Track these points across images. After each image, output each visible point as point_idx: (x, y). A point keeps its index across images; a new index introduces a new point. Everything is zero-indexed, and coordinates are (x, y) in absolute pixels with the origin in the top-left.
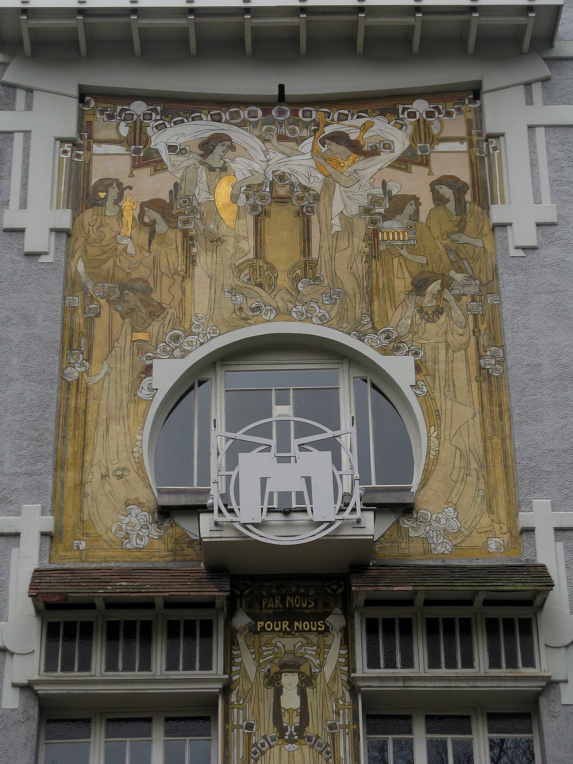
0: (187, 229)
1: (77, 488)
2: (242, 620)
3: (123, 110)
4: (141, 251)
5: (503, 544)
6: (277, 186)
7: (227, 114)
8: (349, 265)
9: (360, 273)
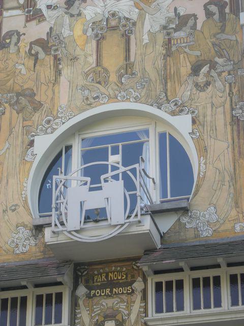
2: (82, 291)
4: (29, 71)
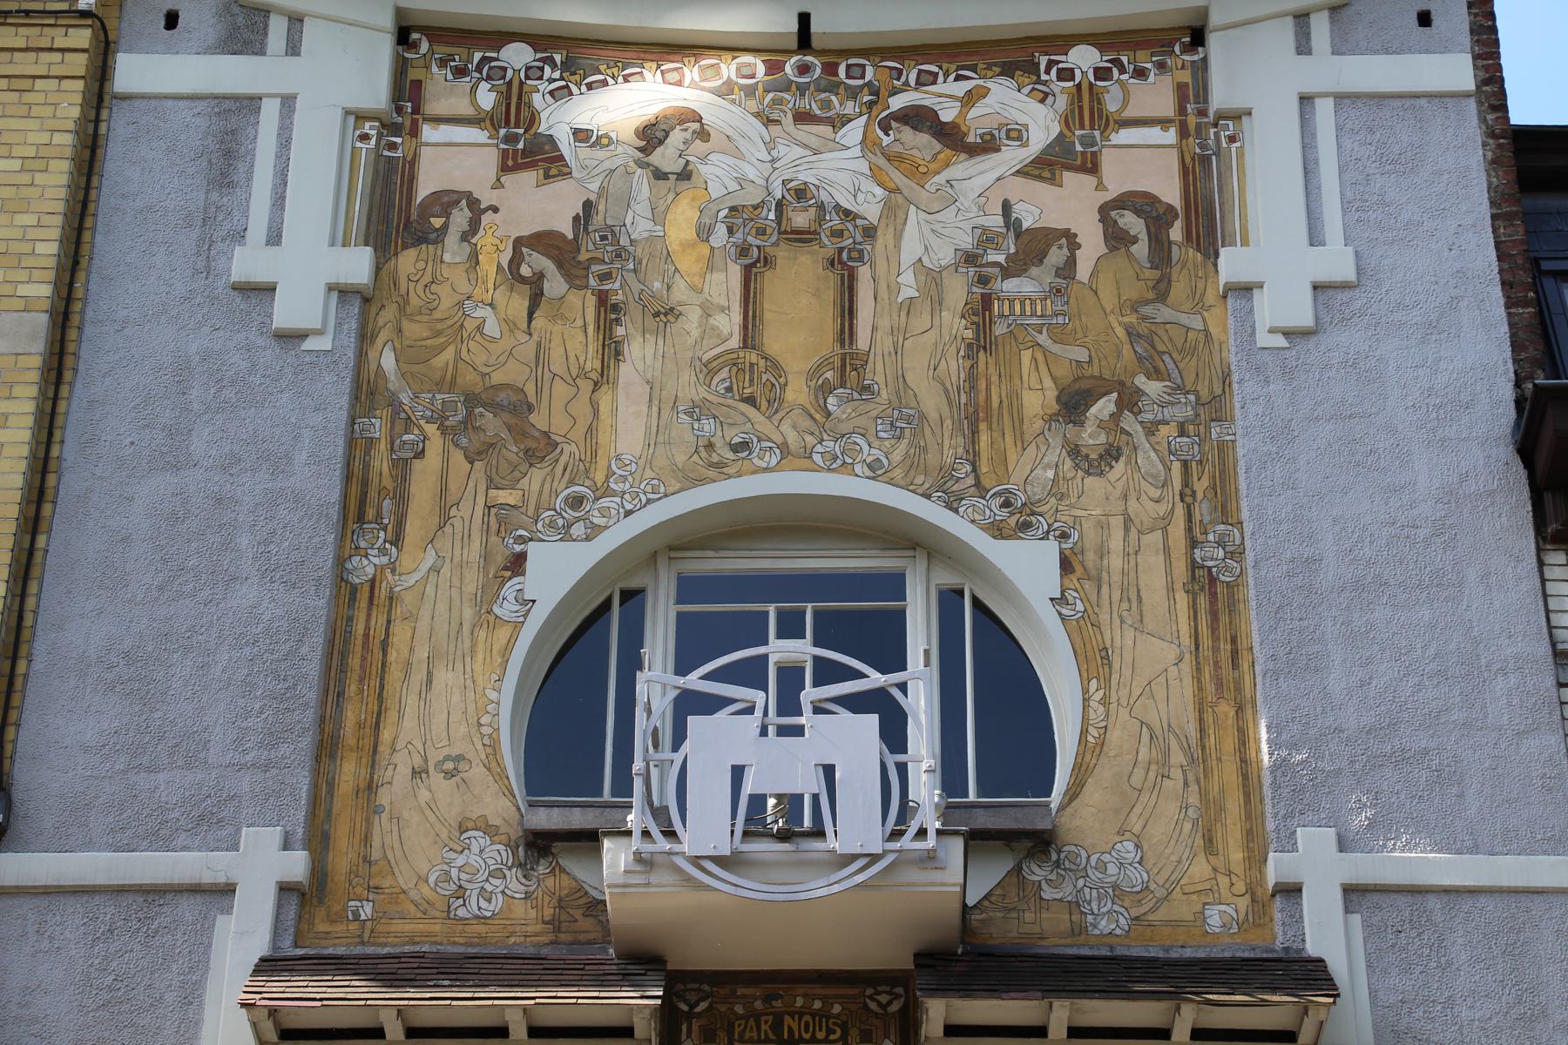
0: (608, 291)
1: (360, 795)
3: (484, 60)
5: (1235, 917)
6: (790, 209)
8: (932, 363)
9: (954, 379)
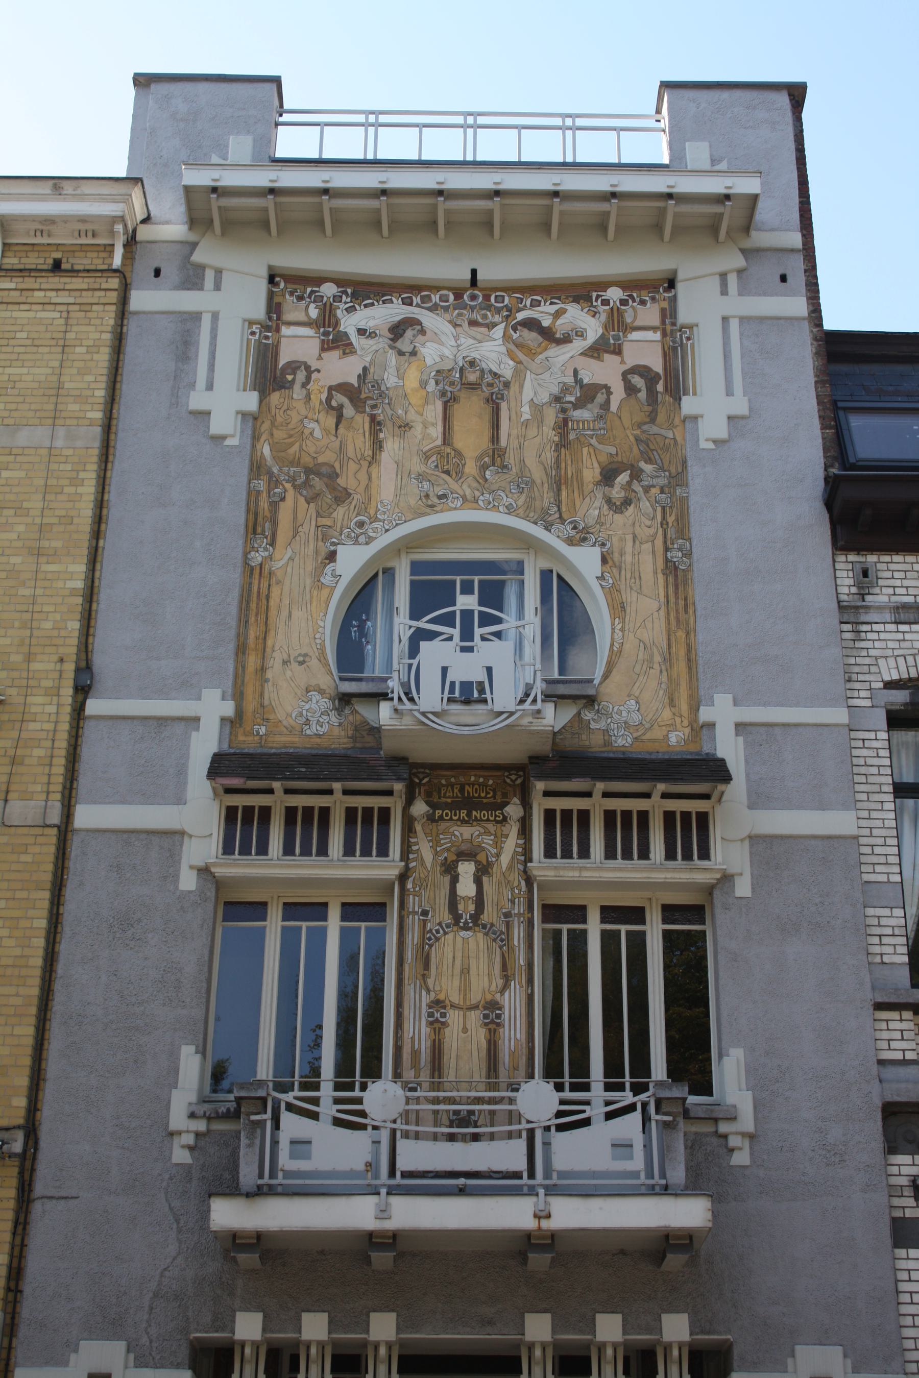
0: (375, 415)
2: (420, 808)
3: (312, 292)
4: (327, 435)
7: (419, 297)
9: (549, 462)
